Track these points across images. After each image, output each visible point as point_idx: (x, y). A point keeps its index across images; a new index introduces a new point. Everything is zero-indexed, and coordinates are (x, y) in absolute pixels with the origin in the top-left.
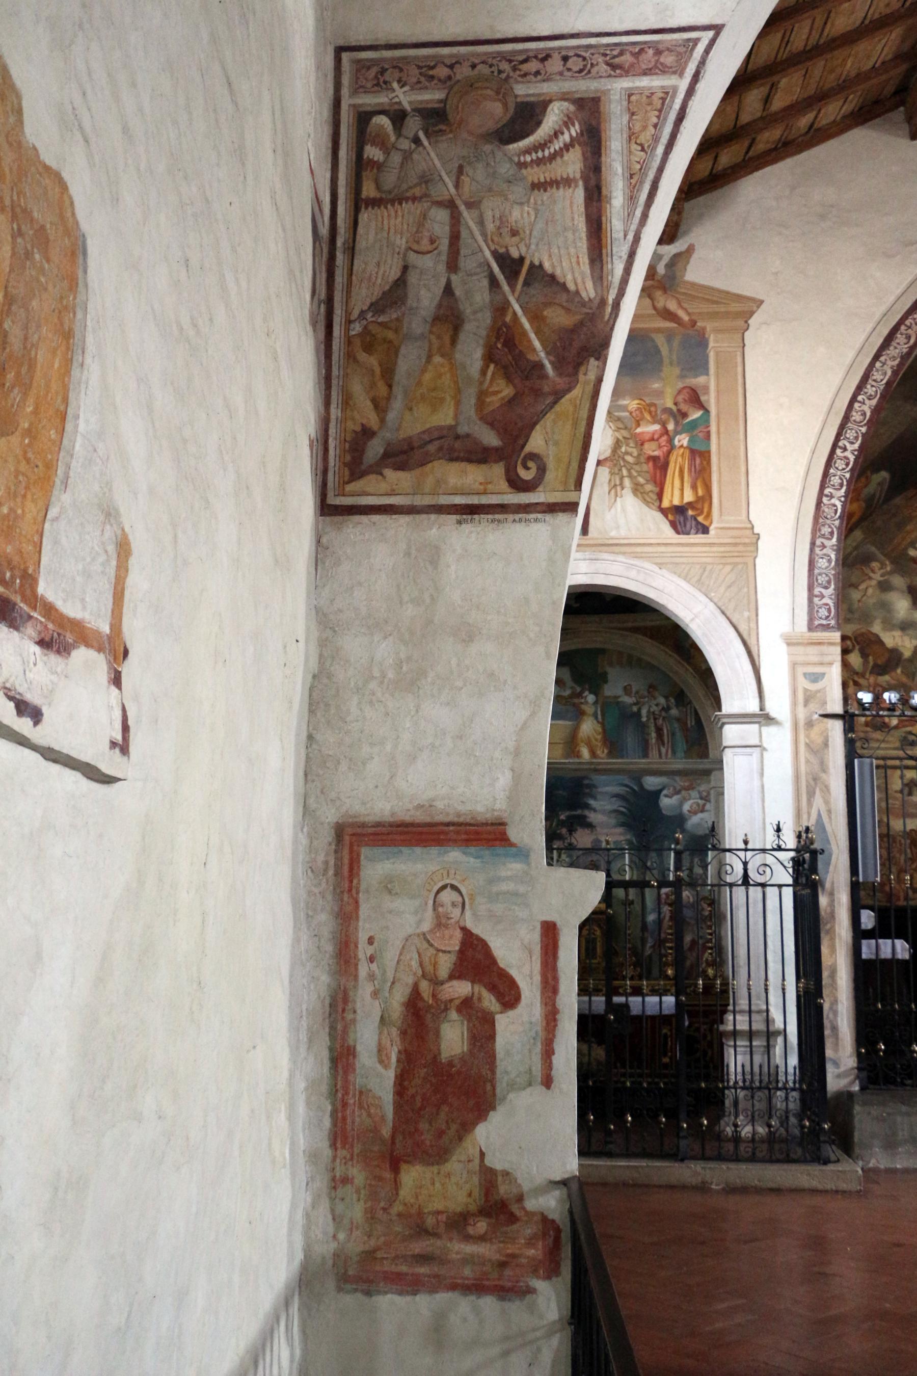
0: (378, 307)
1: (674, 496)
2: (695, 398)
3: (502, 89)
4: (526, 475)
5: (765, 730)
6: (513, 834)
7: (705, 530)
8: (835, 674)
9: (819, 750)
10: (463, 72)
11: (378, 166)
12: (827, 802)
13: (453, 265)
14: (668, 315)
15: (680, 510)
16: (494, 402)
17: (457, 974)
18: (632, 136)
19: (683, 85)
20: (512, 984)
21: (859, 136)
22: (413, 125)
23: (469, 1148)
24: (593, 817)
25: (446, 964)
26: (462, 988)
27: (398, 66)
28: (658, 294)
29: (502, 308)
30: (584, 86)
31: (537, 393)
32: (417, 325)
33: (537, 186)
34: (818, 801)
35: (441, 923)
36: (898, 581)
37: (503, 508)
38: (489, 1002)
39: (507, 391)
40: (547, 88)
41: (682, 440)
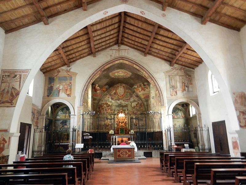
0: (2, 91)
1: (68, 93)
2: (71, 83)
3: (14, 74)
4: (12, 104)
5: (75, 116)
6: (8, 131)
7: (71, 96)
8: (82, 110)
9: (80, 118)
10: (11, 72)
11: (4, 80)
12: (80, 123)
13: (9, 88)
14: (69, 75)
15: (68, 94)
16: (10, 98)
17: (3, 141)
18: (23, 78)
19: (28, 74)
20: (6, 141)
21: (89, 57)
22: (7, 76)
23: (2, 153)
24: (67, 124)
25: (2, 140)
26: (3, 142)
27: (6, 71)
28: (68, 72)
29: (12, 91)
30: (20, 74)
31: (14, 98)
32: (5, 92)
33: (16, 82)
34: (79, 123)
35: (2, 137)
36: (110, 97)
37: (10, 107)
38: (5, 143)
39: (11, 98)
40: (17, 74)
41: (69, 87)
